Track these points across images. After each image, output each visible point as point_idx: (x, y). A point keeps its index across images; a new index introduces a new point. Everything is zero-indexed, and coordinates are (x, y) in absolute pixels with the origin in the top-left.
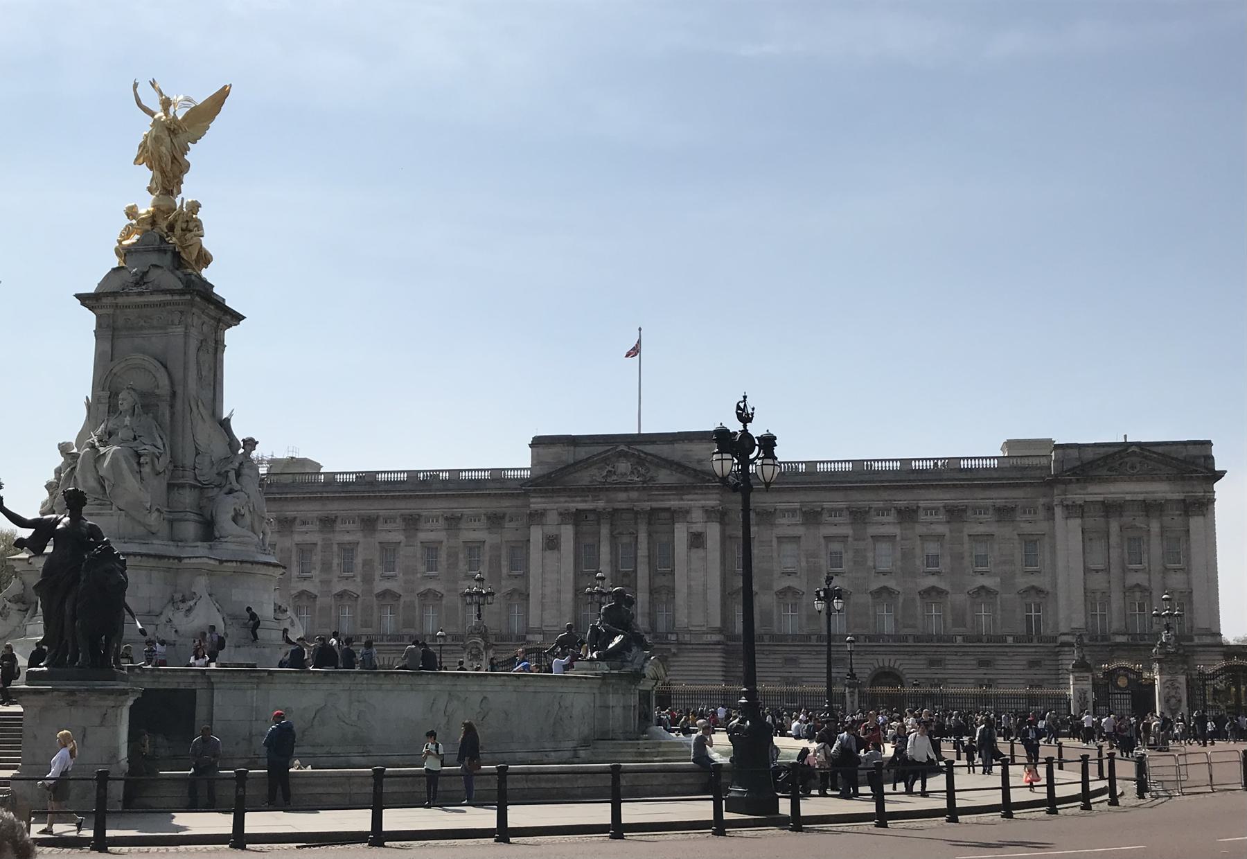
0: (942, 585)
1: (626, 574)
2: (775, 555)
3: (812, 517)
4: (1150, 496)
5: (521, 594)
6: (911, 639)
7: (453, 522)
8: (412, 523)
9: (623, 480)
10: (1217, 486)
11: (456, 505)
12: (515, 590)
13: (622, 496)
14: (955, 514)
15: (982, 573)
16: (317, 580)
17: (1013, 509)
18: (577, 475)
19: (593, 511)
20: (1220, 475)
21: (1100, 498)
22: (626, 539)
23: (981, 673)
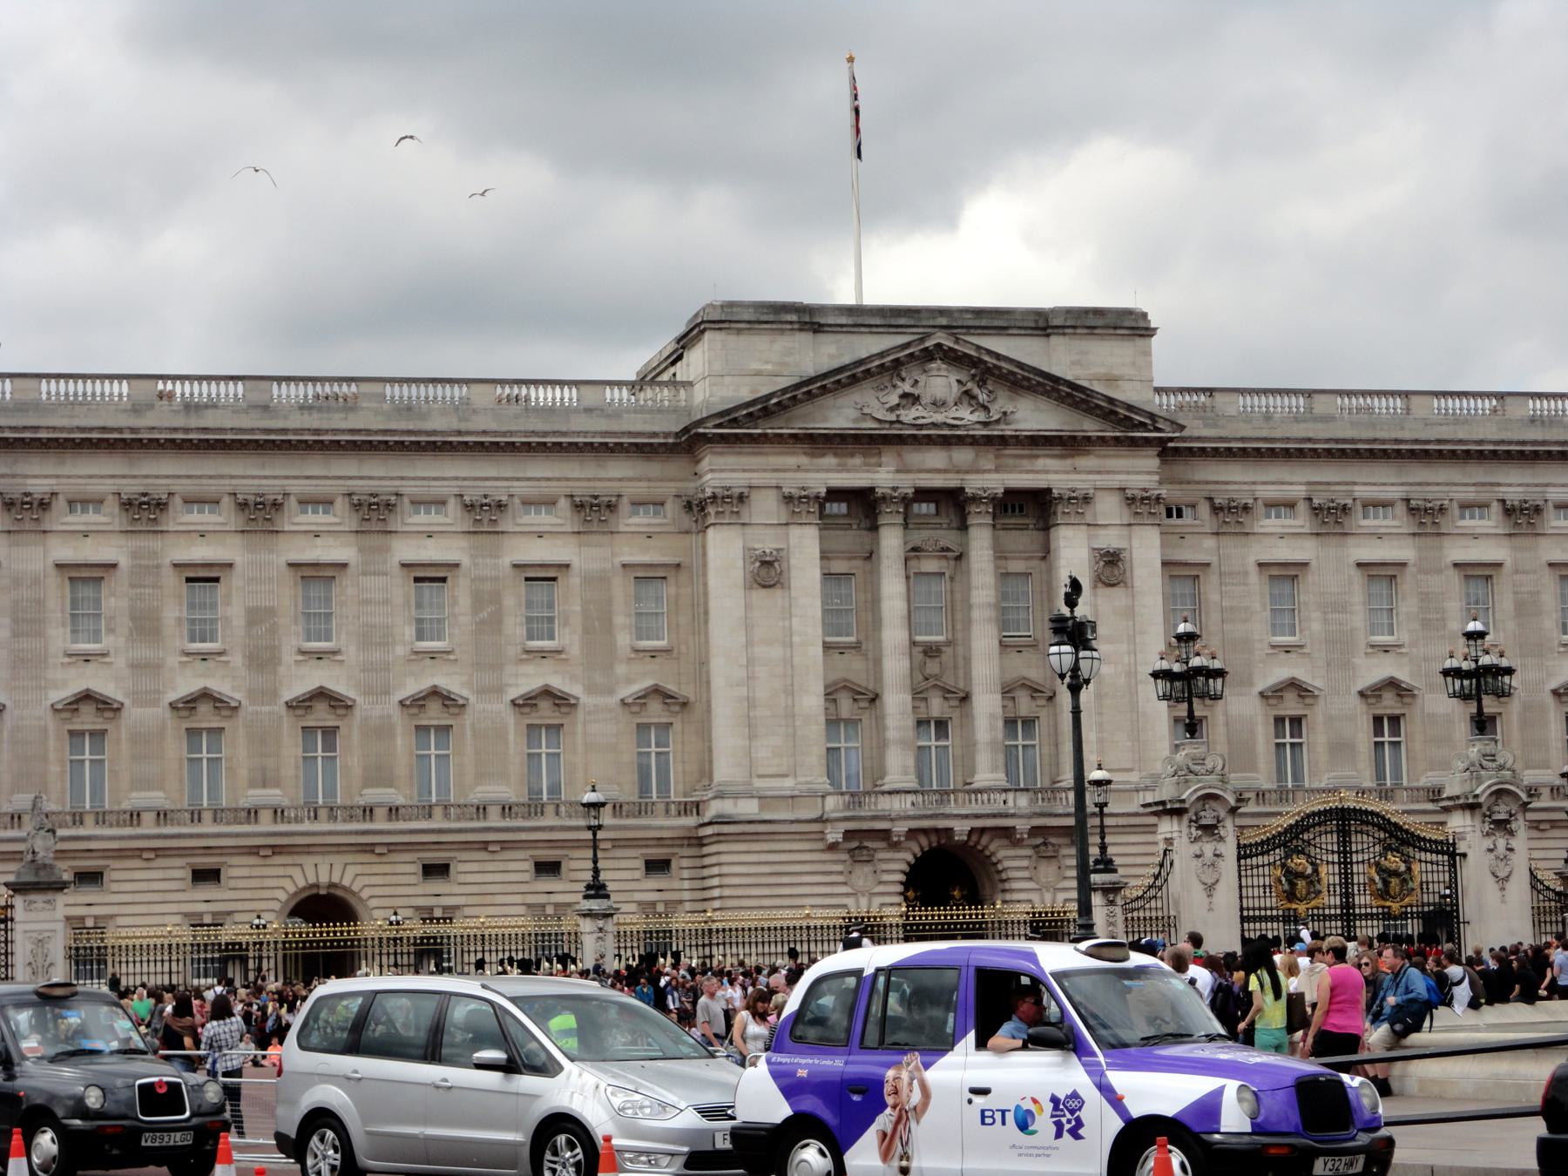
1: (931, 651)
2: (1257, 606)
3: (1331, 517)
7: (485, 514)
8: (374, 512)
9: (939, 418)
11: (492, 473)
12: (657, 692)
13: (935, 458)
16: (120, 662)
18: (828, 401)
22: (930, 565)
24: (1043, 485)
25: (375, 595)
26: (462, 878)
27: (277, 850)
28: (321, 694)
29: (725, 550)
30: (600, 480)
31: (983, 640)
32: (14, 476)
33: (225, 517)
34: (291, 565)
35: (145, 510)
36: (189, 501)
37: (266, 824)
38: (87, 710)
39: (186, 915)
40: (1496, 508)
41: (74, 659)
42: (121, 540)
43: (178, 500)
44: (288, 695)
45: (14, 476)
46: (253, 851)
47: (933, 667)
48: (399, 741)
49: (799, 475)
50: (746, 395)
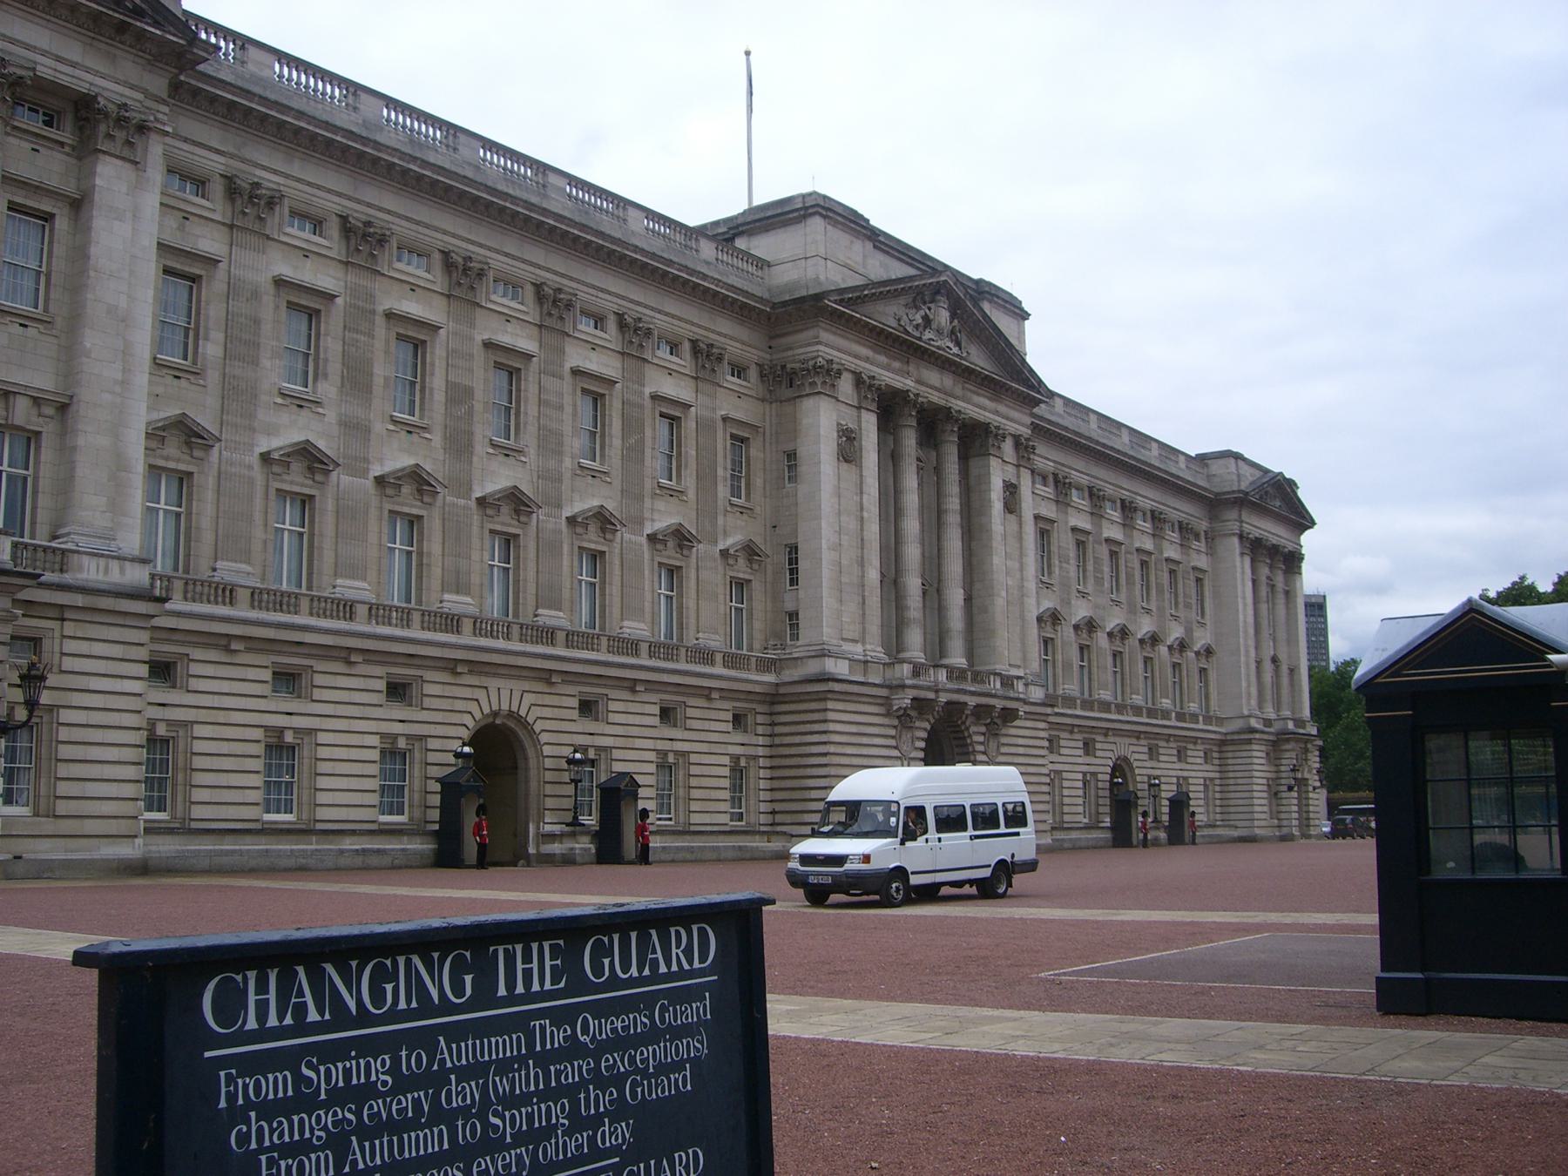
10: (1307, 539)
13: (933, 376)
15: (1176, 618)
16: (331, 415)
21: (1256, 533)
24: (982, 419)
26: (613, 718)
27: (476, 667)
29: (822, 419)
30: (713, 331)
32: (244, 160)
34: (489, 345)
37: (467, 639)
39: (383, 735)
41: (289, 400)
42: (341, 274)
45: (244, 160)
46: (451, 666)
48: (566, 562)
49: (867, 366)
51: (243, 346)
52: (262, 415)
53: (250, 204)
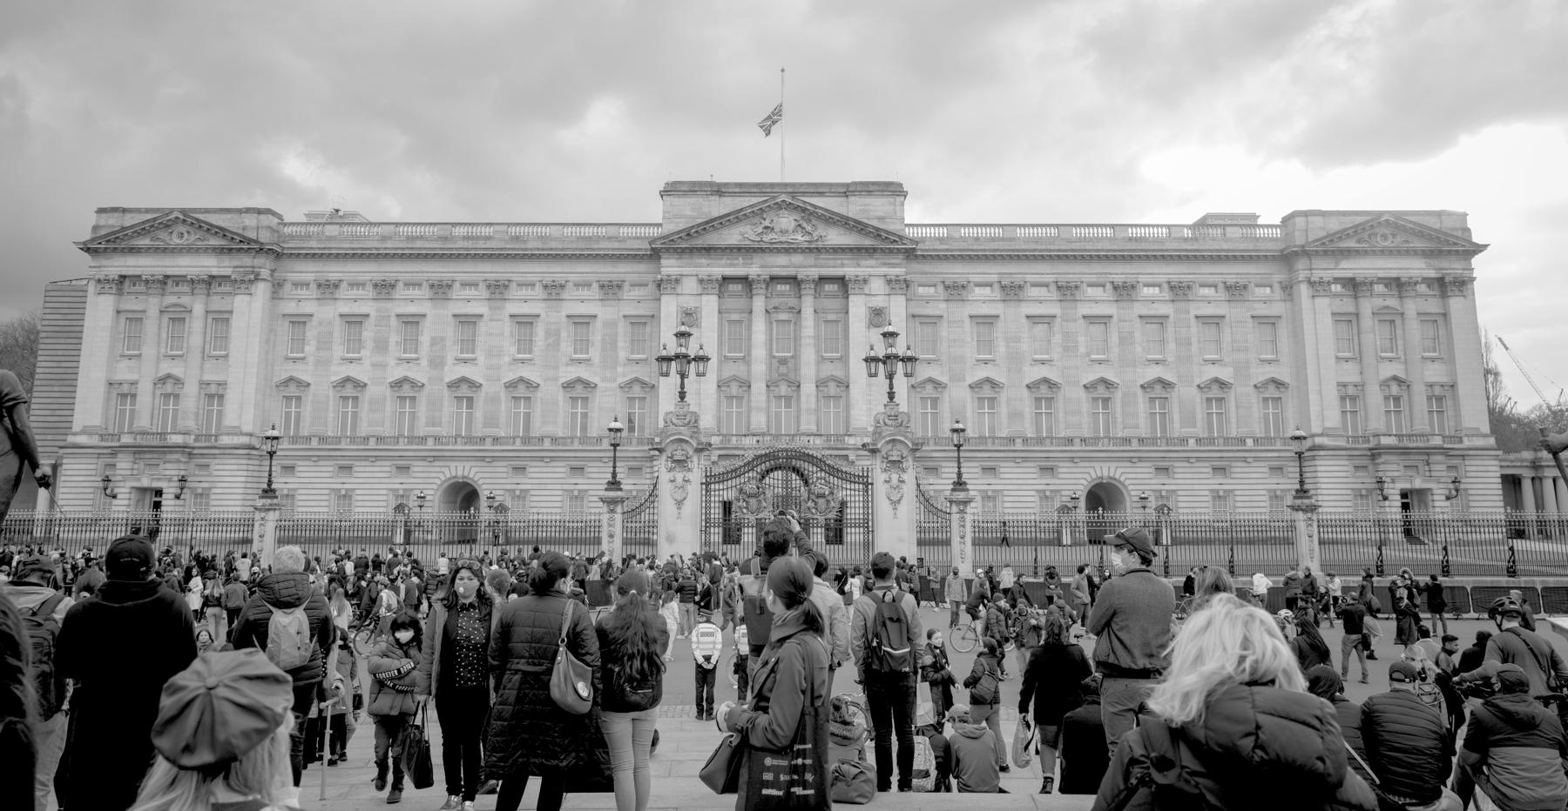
0: (1169, 377)
1: (783, 361)
3: (1012, 291)
4: (1404, 275)
5: (643, 384)
6: (1135, 442)
7: (554, 290)
8: (498, 289)
12: (637, 380)
13: (782, 260)
14: (1179, 291)
15: (1214, 362)
17: (1245, 287)
19: (744, 280)
20: (1479, 248)
21: (1349, 274)
22: (783, 316)
23: (1216, 482)
25: (496, 332)
28: (464, 380)
31: (808, 355)
33: (425, 292)
35: (384, 288)
36: (407, 285)
38: (349, 386)
40: (1109, 286)
43: (400, 285)
44: (447, 380)
46: (424, 458)
47: (783, 369)
50: (682, 227)
51: (325, 343)
52: (333, 368)
53: (328, 288)
